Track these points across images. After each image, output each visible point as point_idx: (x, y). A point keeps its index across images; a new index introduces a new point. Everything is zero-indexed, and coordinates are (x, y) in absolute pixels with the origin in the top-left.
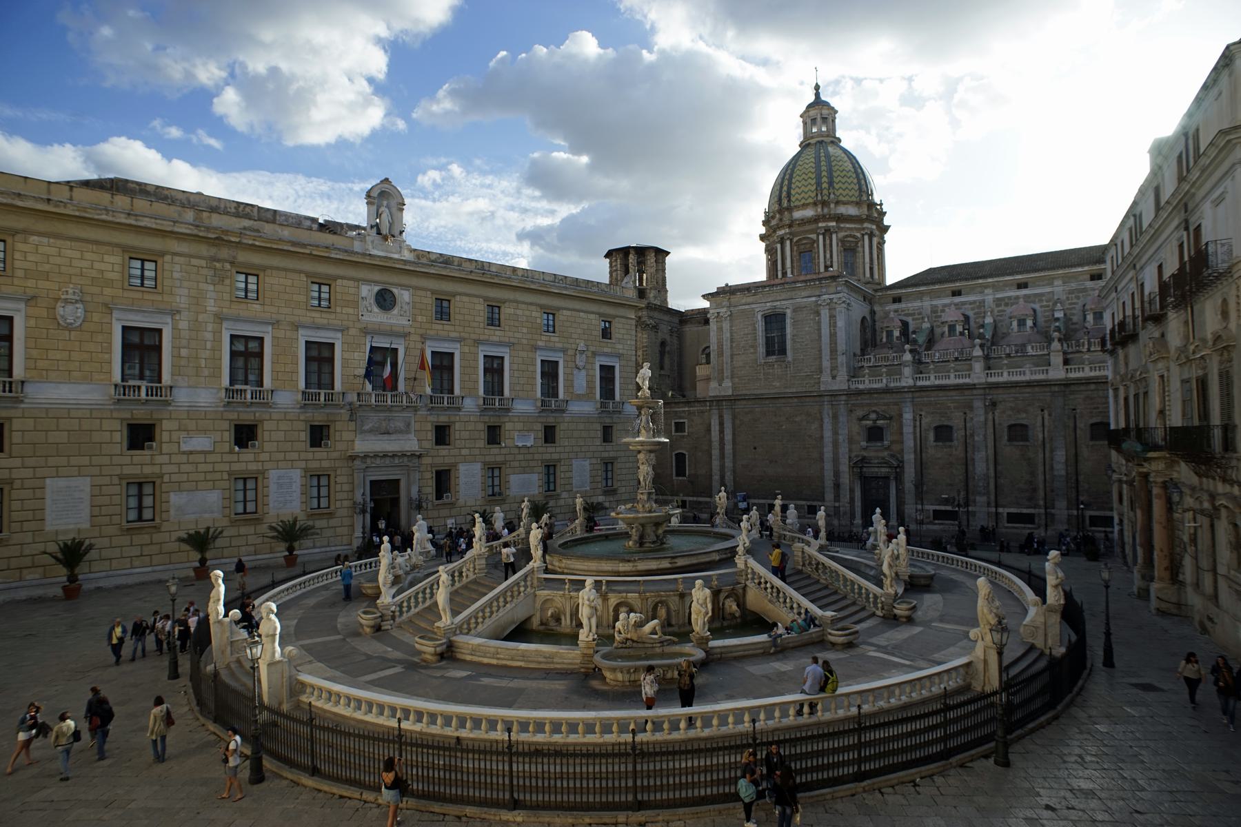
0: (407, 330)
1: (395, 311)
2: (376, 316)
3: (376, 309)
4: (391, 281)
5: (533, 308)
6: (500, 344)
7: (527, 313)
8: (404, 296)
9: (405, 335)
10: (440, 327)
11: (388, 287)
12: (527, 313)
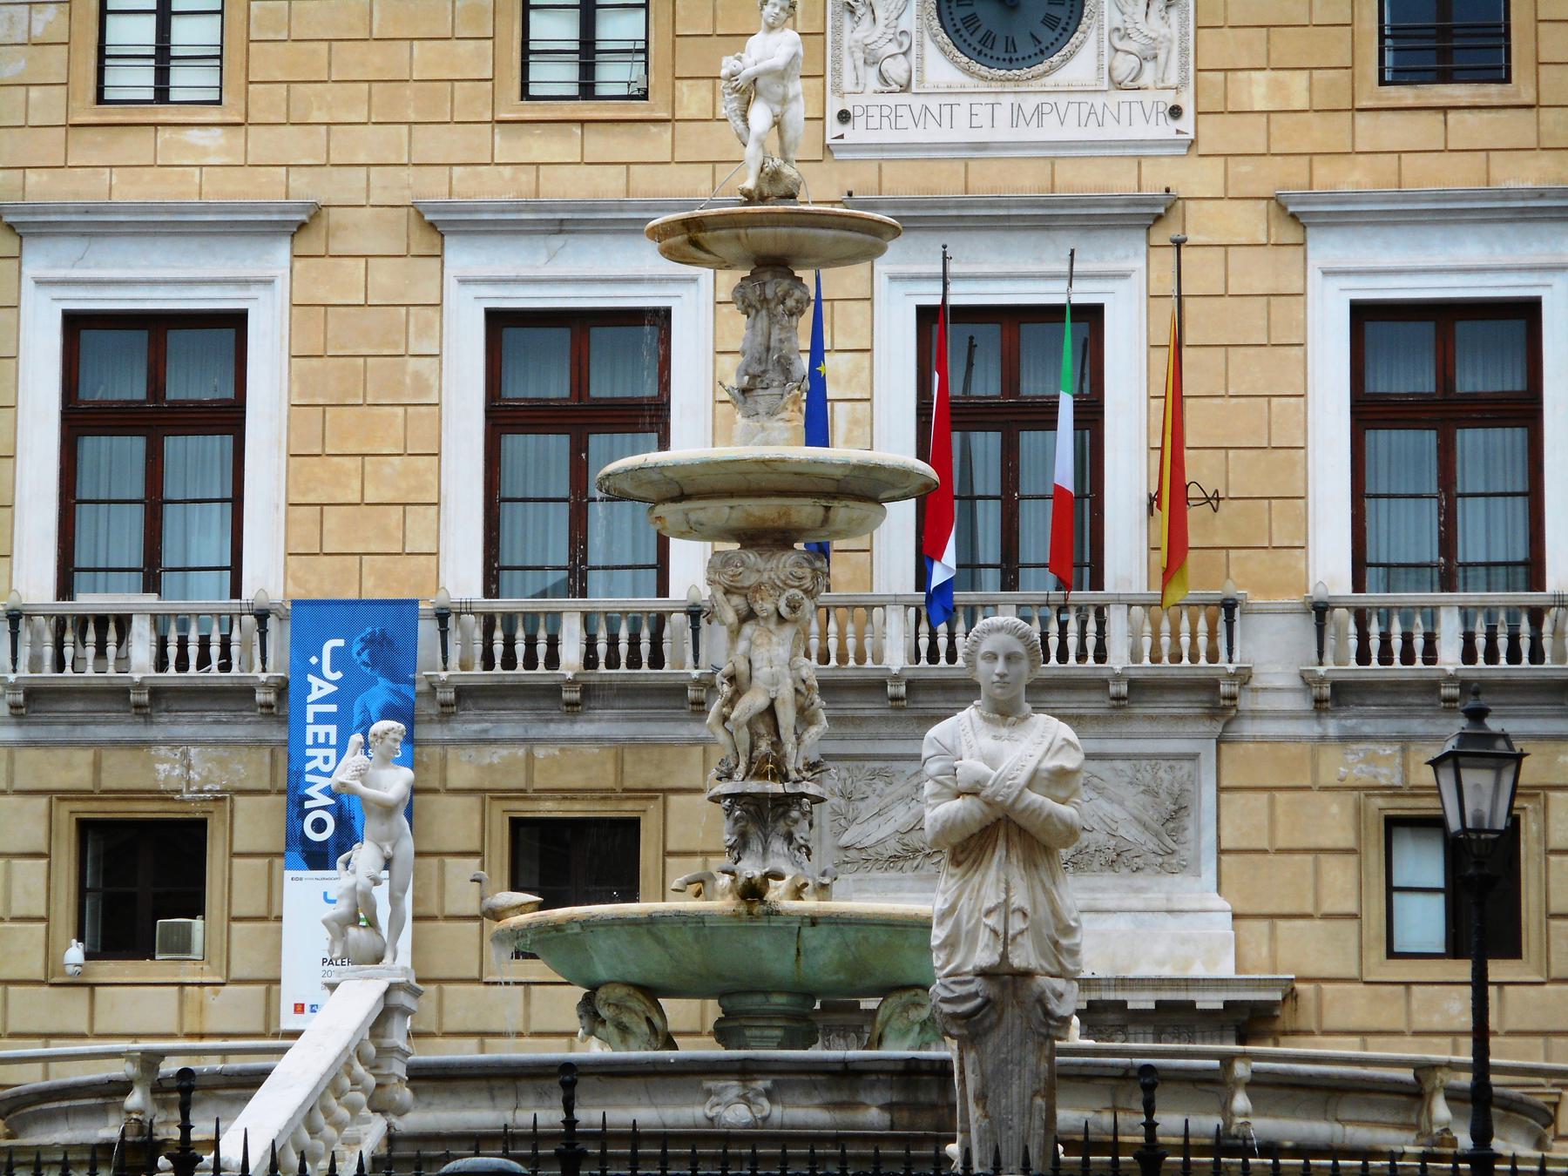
0: (1153, 185)
1: (1081, 62)
3: (941, 67)
9: (1150, 216)
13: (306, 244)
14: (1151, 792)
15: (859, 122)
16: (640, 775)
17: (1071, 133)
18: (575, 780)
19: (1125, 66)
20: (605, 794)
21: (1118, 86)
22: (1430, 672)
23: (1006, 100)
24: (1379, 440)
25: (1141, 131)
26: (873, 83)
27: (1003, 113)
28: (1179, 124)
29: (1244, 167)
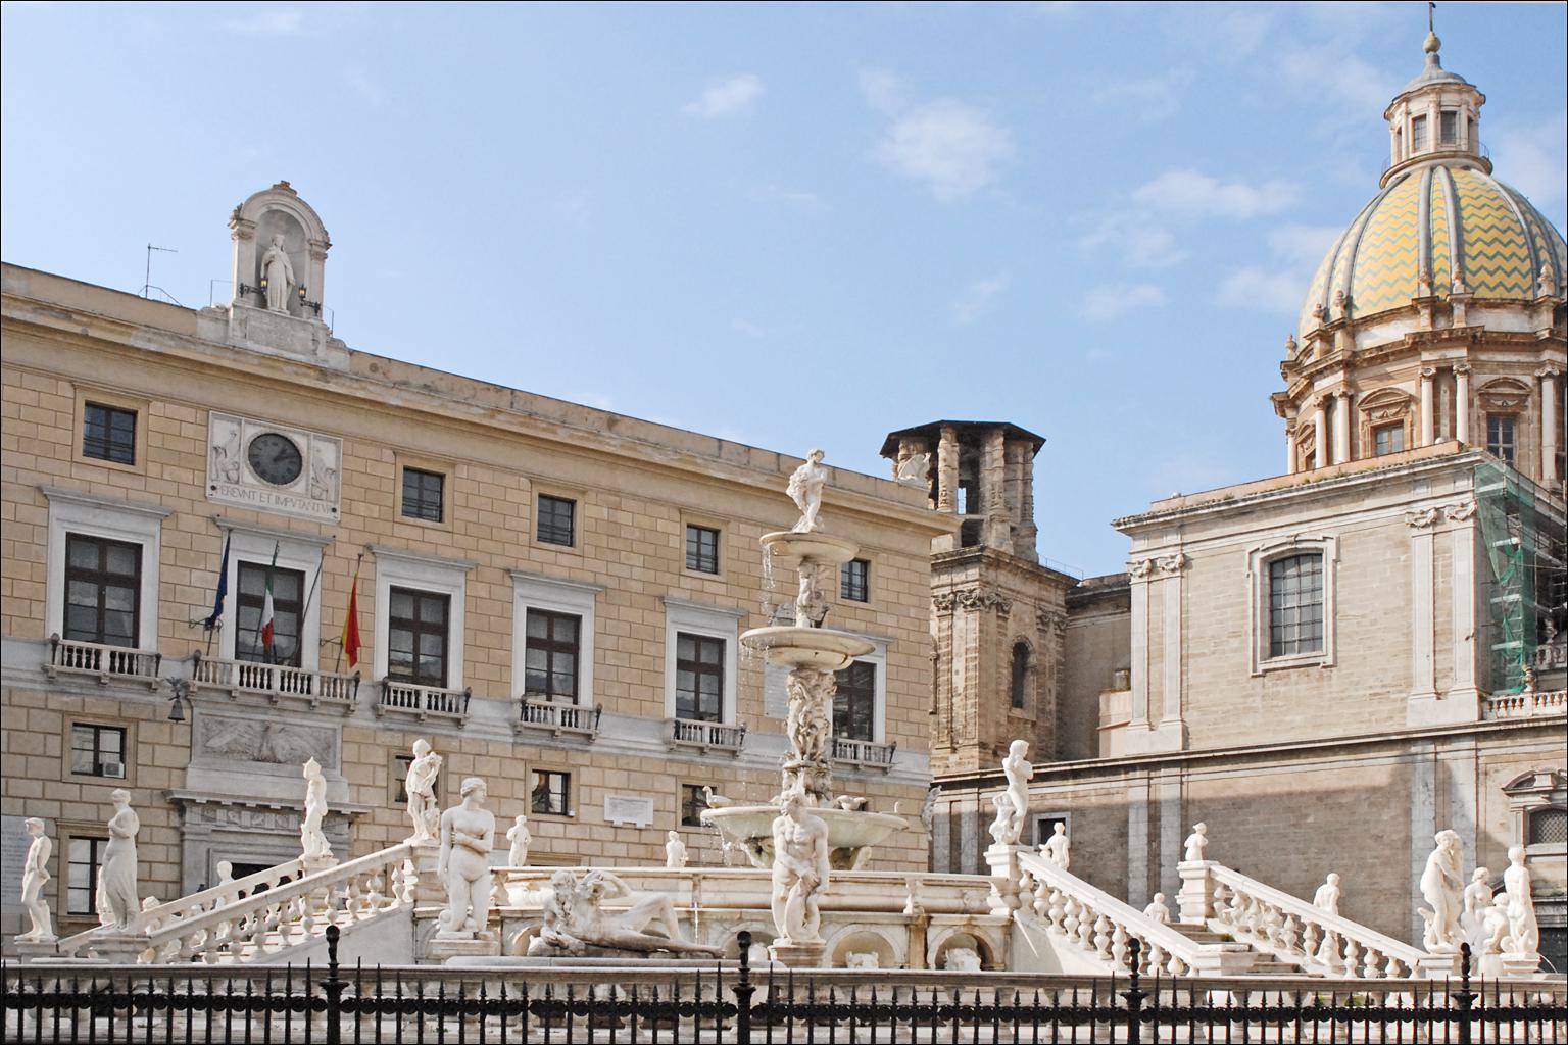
0: (328, 532)
1: (300, 486)
2: (253, 494)
3: (249, 477)
4: (291, 415)
5: (664, 511)
6: (569, 585)
7: (645, 522)
8: (320, 454)
9: (324, 545)
10: (415, 533)
11: (282, 430)
12: (645, 522)
13: (471, 576)
14: (317, 739)
15: (219, 491)
16: (128, 712)
17: (296, 510)
18: (100, 711)
19: (317, 492)
20: (113, 719)
21: (314, 498)
22: (96, 673)
23: (274, 494)
24: (76, 585)
25: (321, 514)
26: (224, 478)
27: (273, 498)
28: (335, 515)
29: (356, 534)
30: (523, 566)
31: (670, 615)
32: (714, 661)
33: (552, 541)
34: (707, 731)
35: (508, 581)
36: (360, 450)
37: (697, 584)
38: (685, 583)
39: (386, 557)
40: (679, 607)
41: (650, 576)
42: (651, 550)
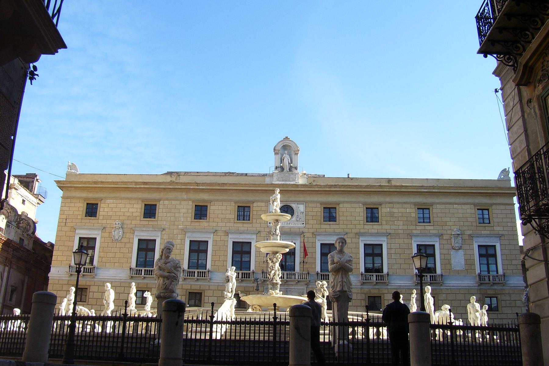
0: (301, 230)
5: (408, 206)
6: (378, 234)
7: (403, 210)
8: (300, 208)
10: (328, 226)
12: (403, 210)
17: (292, 225)
19: (298, 219)
30: (362, 231)
31: (187, 235)
32: (432, 252)
33: (372, 222)
34: (429, 277)
35: (357, 237)
36: (310, 205)
37: (423, 228)
38: (418, 228)
39: (319, 235)
40: (417, 235)
41: (405, 227)
42: (405, 219)
